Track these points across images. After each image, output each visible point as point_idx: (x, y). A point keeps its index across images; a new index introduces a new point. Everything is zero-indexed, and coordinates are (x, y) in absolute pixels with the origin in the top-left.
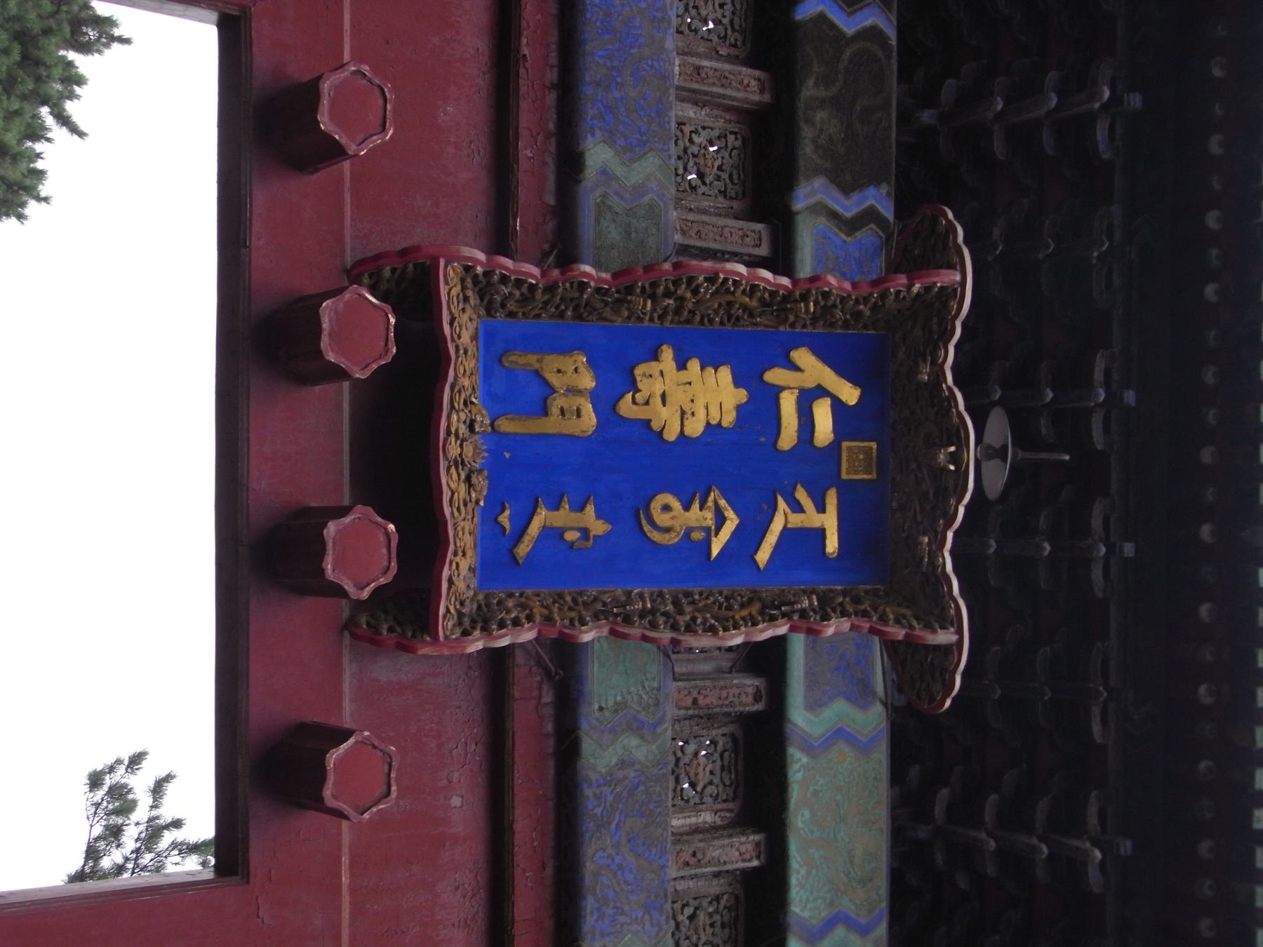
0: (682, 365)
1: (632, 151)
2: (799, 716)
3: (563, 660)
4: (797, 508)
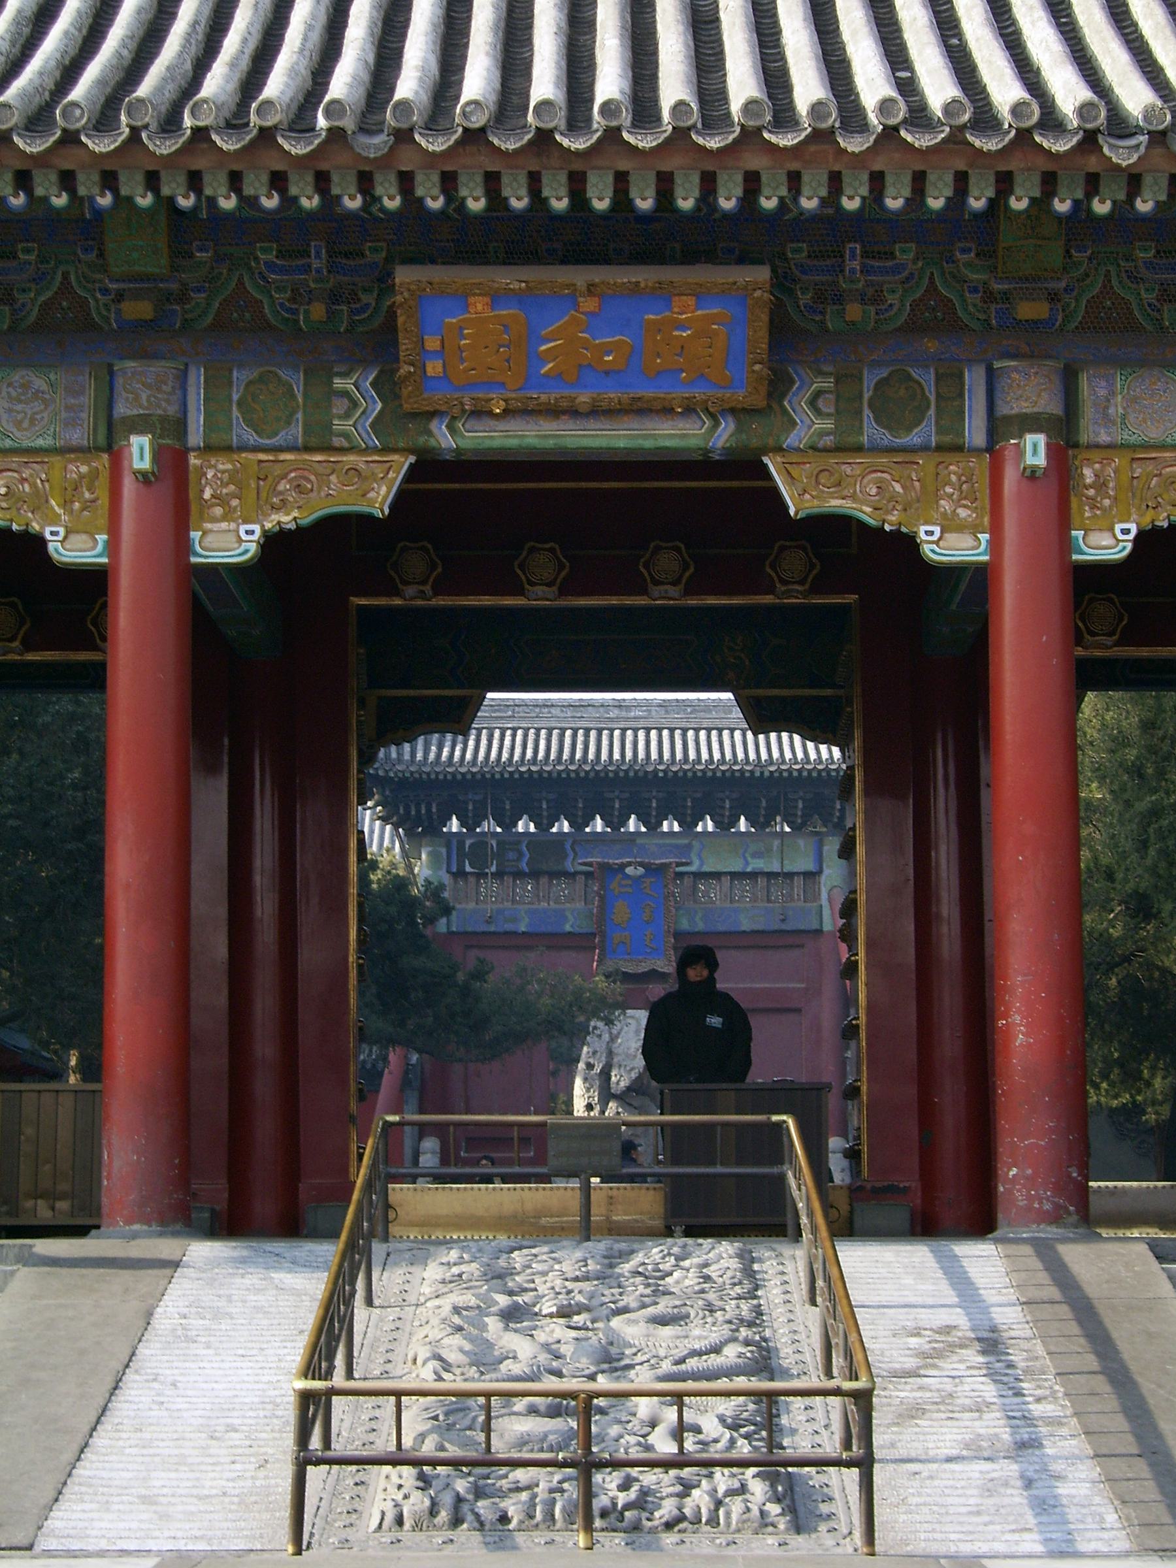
1: (565, 919)
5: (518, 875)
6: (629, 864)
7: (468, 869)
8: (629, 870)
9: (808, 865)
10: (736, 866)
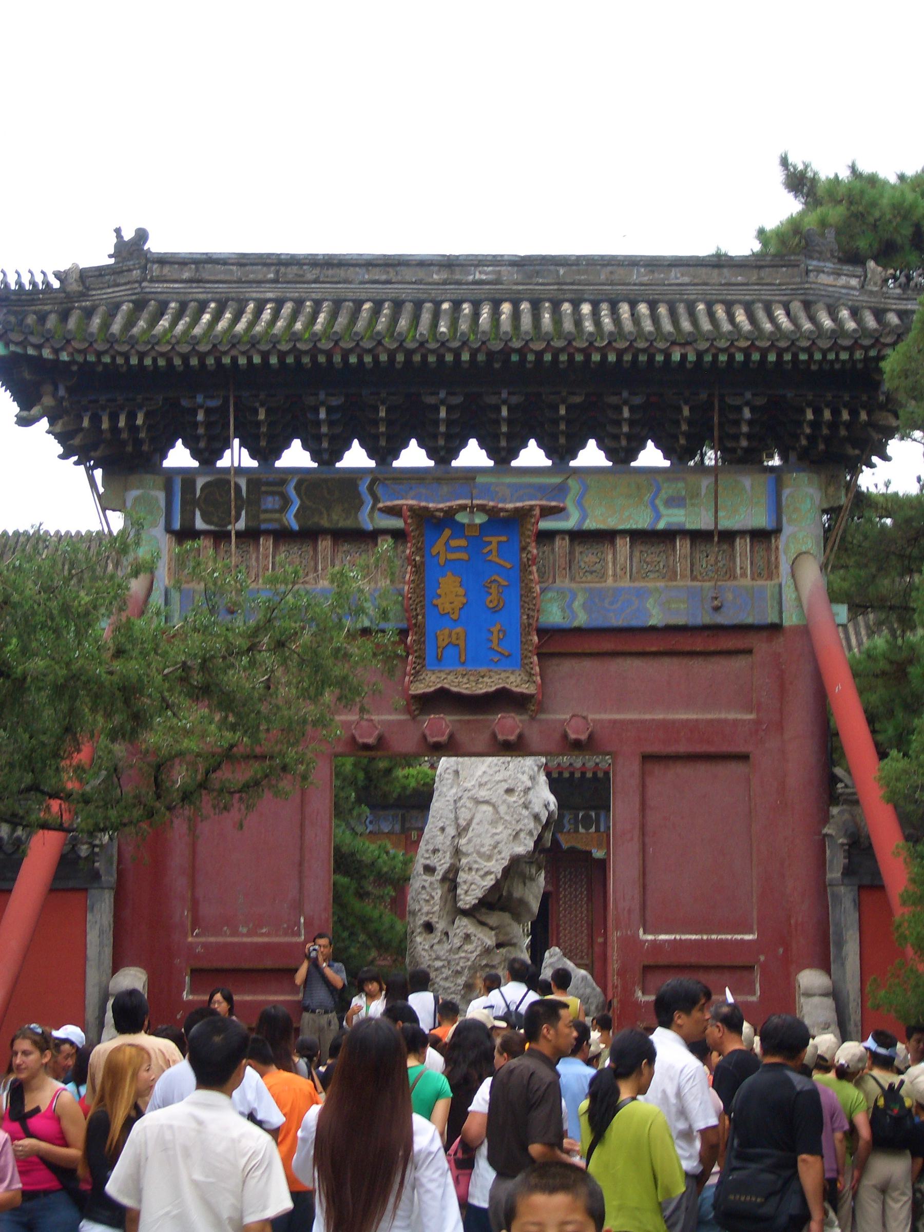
0: (440, 596)
2: (570, 524)
3: (546, 633)
4: (491, 551)
5: (282, 536)
6: (463, 508)
7: (200, 524)
8: (462, 518)
9: (760, 519)
10: (641, 520)
